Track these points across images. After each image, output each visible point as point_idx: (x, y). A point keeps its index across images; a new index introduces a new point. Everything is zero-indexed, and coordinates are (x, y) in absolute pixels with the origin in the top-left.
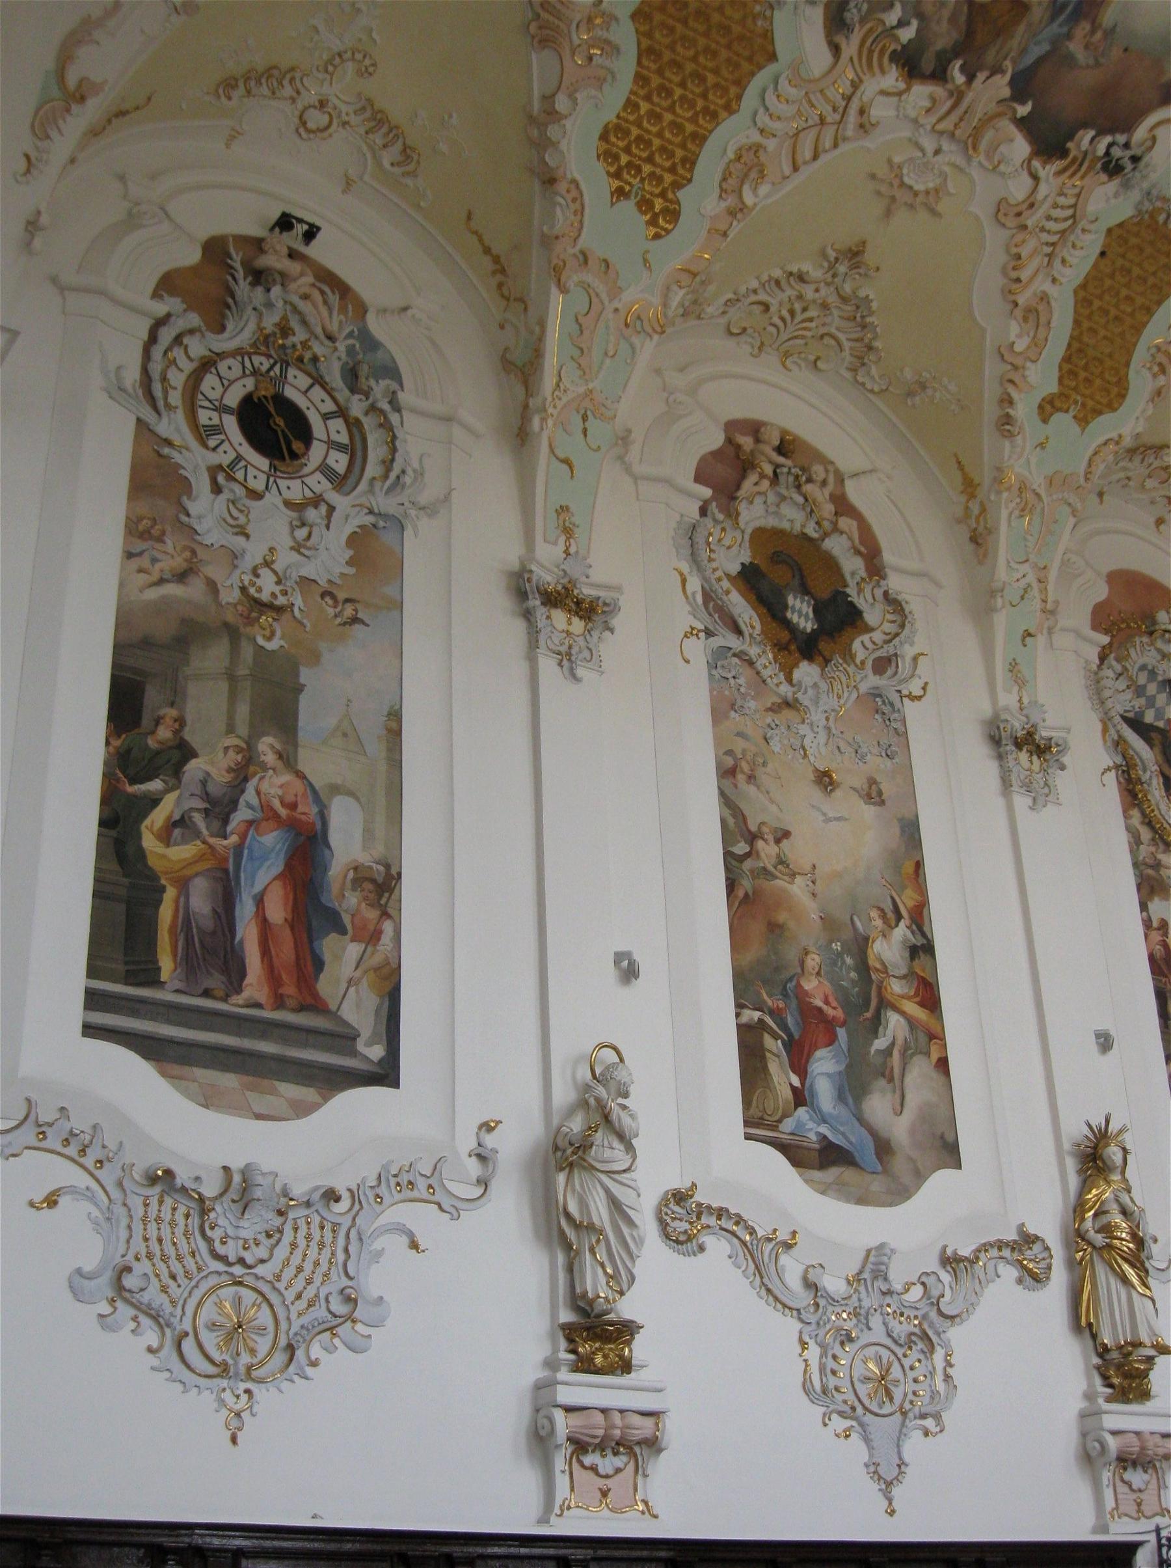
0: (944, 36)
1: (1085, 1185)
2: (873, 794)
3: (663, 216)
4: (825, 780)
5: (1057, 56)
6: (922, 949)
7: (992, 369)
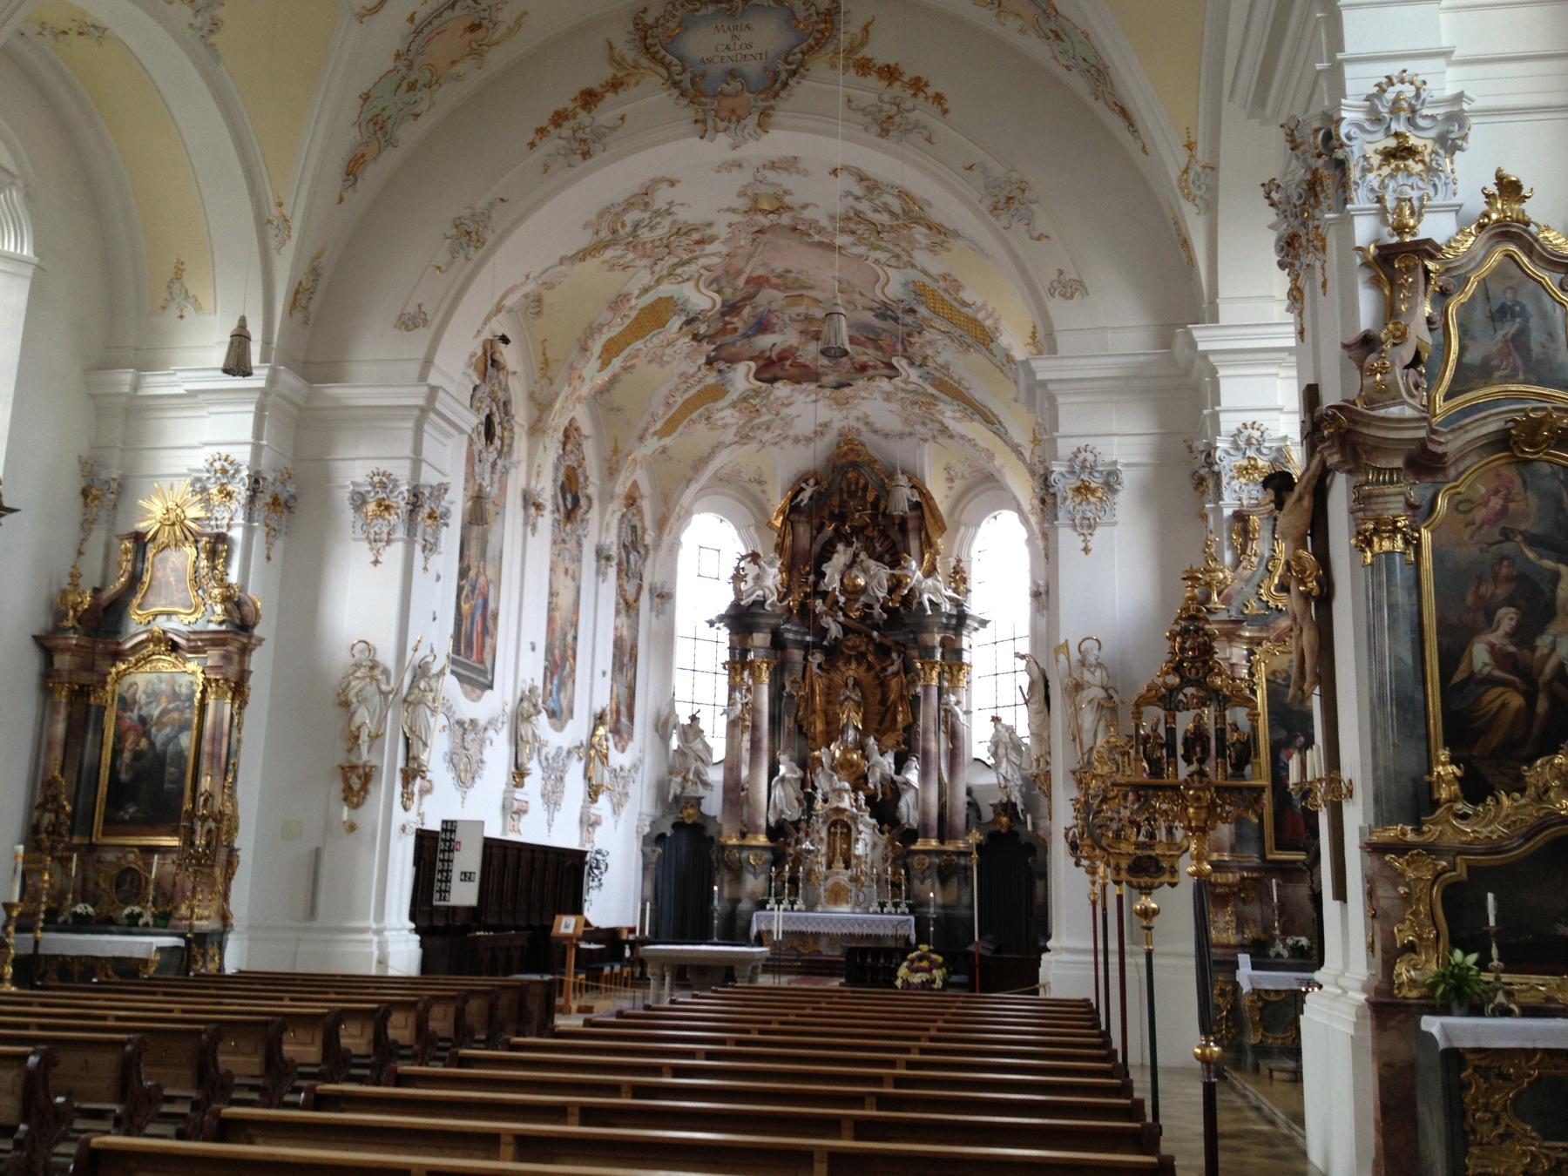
0: (711, 331)
1: (595, 728)
2: (574, 579)
3: (605, 364)
4: (566, 572)
5: (733, 344)
6: (575, 638)
7: (647, 418)
